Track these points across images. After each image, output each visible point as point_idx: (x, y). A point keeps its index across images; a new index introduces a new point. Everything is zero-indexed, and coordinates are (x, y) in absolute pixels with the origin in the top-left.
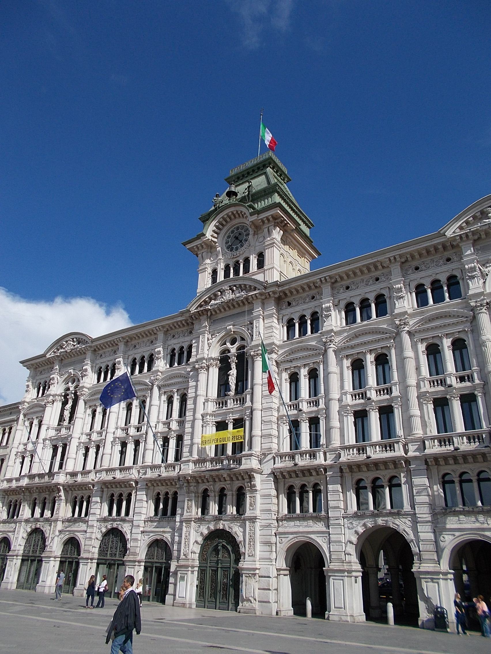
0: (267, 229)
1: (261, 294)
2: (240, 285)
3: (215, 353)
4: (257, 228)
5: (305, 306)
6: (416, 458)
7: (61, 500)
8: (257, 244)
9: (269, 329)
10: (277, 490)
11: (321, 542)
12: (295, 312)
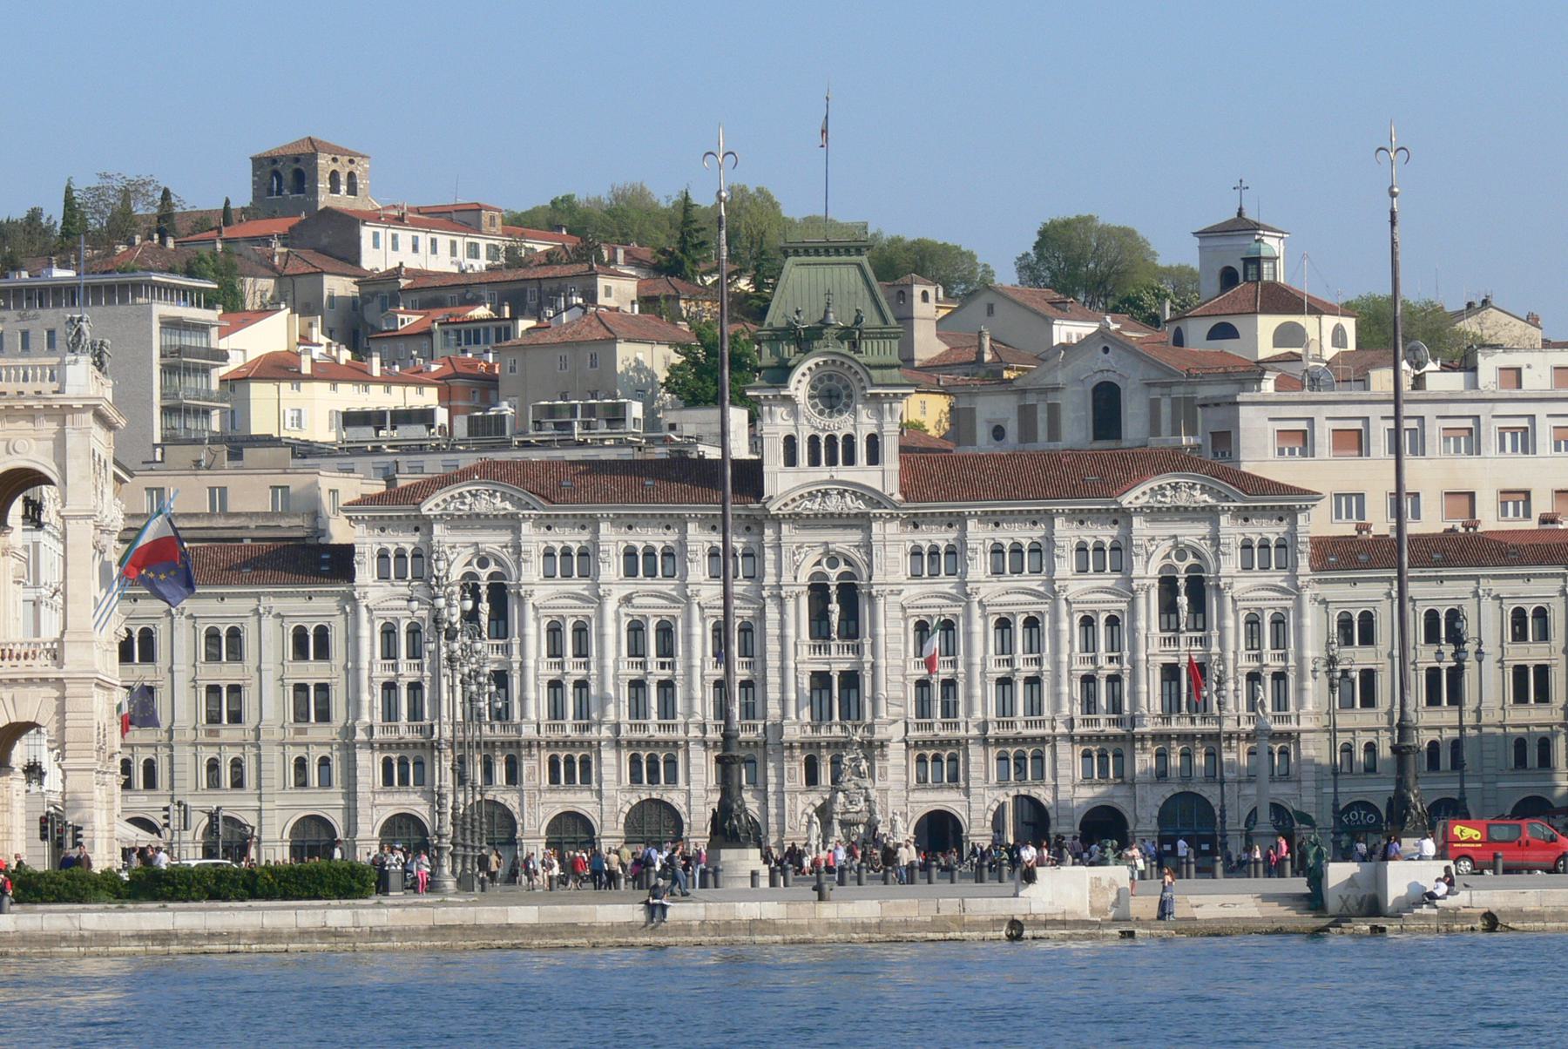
6: (1063, 735)
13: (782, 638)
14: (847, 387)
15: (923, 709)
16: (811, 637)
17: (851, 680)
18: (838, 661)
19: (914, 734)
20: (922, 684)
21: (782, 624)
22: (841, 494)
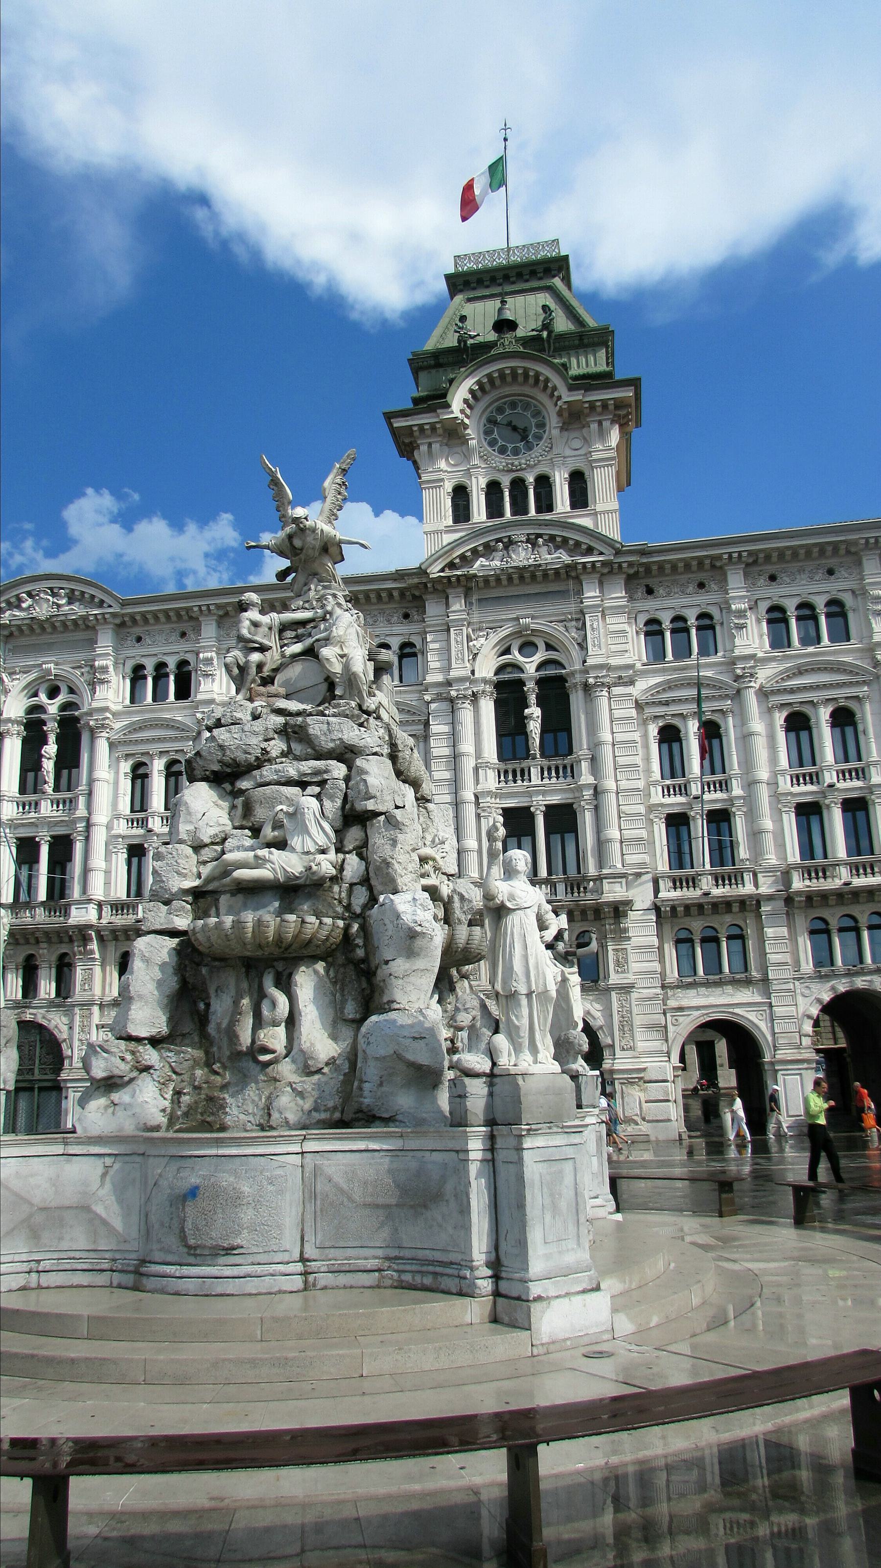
0: (596, 425)
1: (604, 564)
2: (552, 538)
3: (487, 667)
4: (574, 418)
5: (685, 601)
7: (94, 959)
8: (568, 452)
9: (612, 636)
10: (660, 935)
11: (756, 1021)
12: (665, 609)
13: (455, 758)
14: (537, 413)
15: (680, 854)
16: (501, 757)
17: (563, 819)
18: (541, 791)
19: (667, 893)
20: (677, 822)
21: (454, 738)
22: (532, 541)
